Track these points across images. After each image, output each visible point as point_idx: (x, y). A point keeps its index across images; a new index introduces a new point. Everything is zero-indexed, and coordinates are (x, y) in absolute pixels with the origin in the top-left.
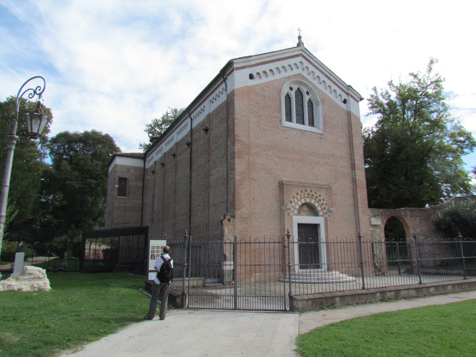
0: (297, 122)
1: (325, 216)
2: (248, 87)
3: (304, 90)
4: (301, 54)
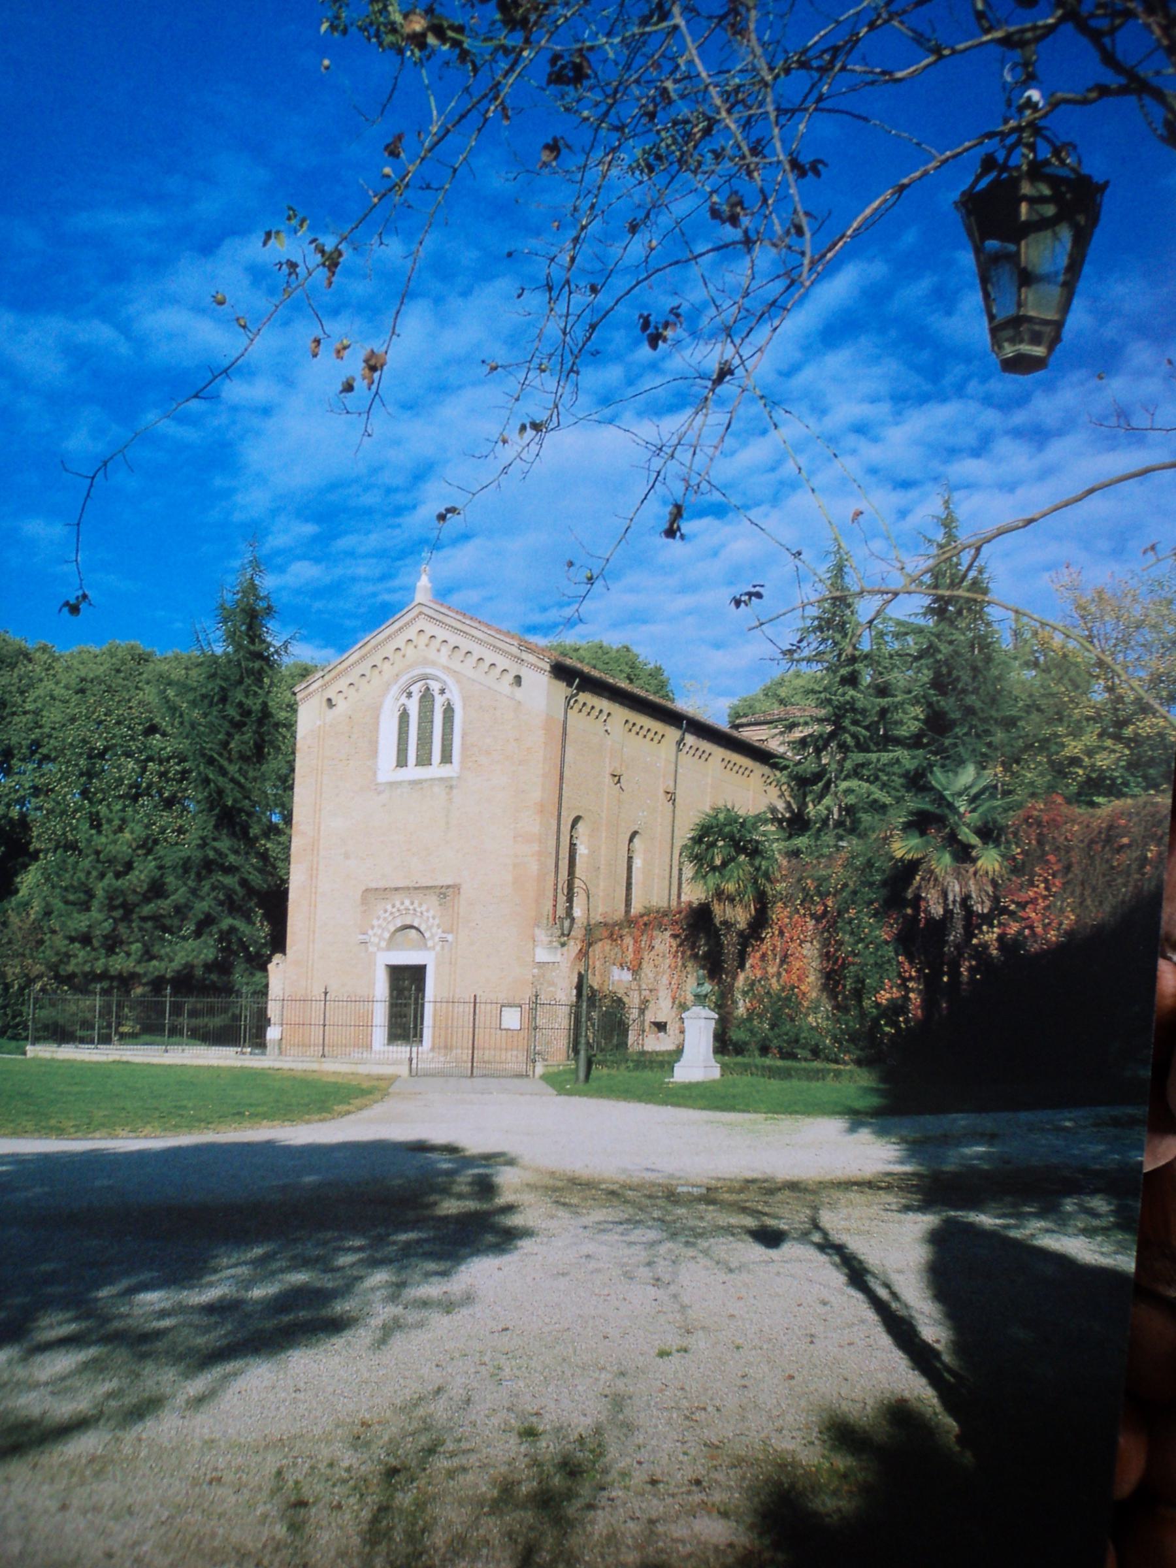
3: (435, 686)
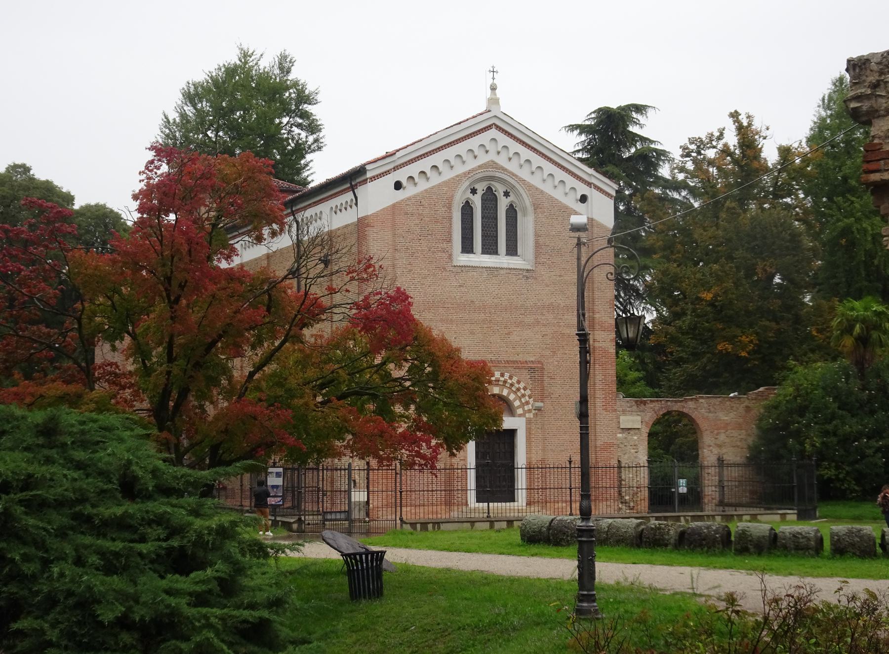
0: (483, 253)
1: (527, 415)
2: (394, 206)
3: (499, 190)
4: (495, 125)
